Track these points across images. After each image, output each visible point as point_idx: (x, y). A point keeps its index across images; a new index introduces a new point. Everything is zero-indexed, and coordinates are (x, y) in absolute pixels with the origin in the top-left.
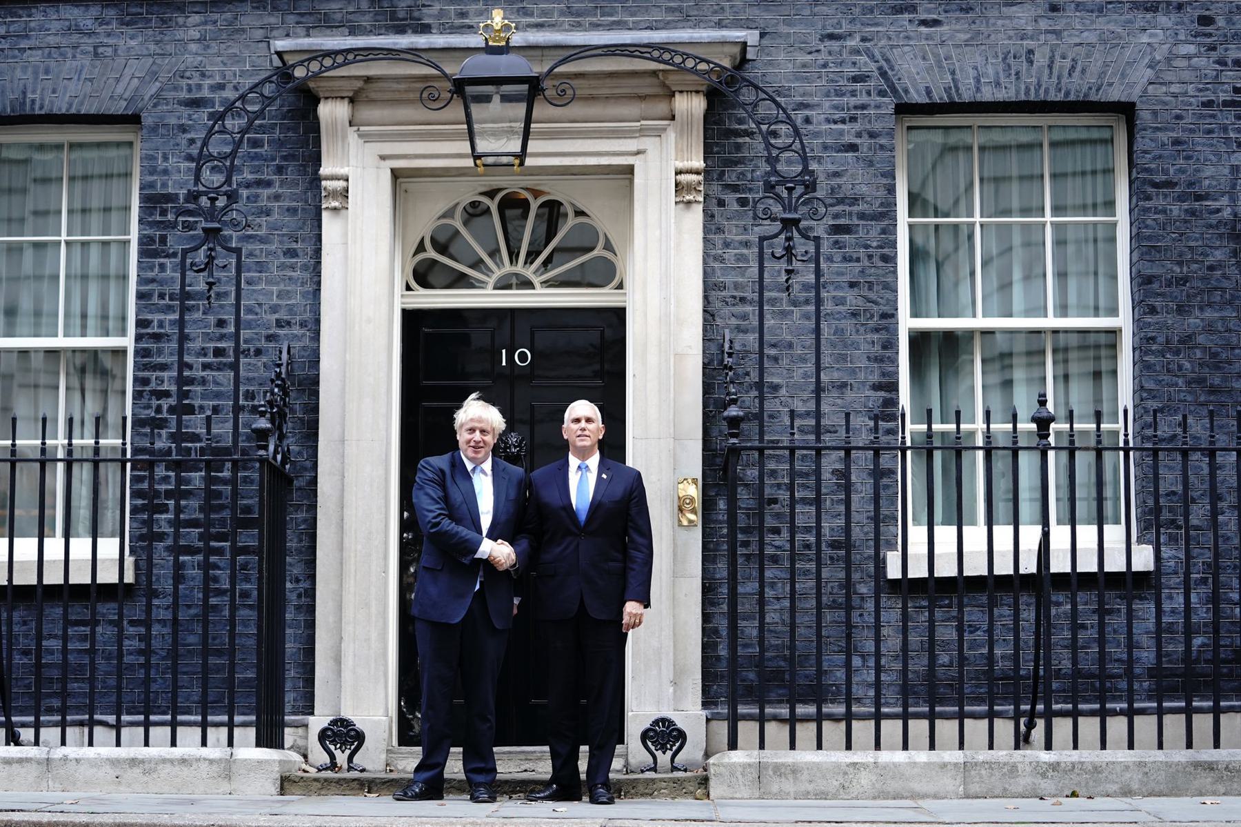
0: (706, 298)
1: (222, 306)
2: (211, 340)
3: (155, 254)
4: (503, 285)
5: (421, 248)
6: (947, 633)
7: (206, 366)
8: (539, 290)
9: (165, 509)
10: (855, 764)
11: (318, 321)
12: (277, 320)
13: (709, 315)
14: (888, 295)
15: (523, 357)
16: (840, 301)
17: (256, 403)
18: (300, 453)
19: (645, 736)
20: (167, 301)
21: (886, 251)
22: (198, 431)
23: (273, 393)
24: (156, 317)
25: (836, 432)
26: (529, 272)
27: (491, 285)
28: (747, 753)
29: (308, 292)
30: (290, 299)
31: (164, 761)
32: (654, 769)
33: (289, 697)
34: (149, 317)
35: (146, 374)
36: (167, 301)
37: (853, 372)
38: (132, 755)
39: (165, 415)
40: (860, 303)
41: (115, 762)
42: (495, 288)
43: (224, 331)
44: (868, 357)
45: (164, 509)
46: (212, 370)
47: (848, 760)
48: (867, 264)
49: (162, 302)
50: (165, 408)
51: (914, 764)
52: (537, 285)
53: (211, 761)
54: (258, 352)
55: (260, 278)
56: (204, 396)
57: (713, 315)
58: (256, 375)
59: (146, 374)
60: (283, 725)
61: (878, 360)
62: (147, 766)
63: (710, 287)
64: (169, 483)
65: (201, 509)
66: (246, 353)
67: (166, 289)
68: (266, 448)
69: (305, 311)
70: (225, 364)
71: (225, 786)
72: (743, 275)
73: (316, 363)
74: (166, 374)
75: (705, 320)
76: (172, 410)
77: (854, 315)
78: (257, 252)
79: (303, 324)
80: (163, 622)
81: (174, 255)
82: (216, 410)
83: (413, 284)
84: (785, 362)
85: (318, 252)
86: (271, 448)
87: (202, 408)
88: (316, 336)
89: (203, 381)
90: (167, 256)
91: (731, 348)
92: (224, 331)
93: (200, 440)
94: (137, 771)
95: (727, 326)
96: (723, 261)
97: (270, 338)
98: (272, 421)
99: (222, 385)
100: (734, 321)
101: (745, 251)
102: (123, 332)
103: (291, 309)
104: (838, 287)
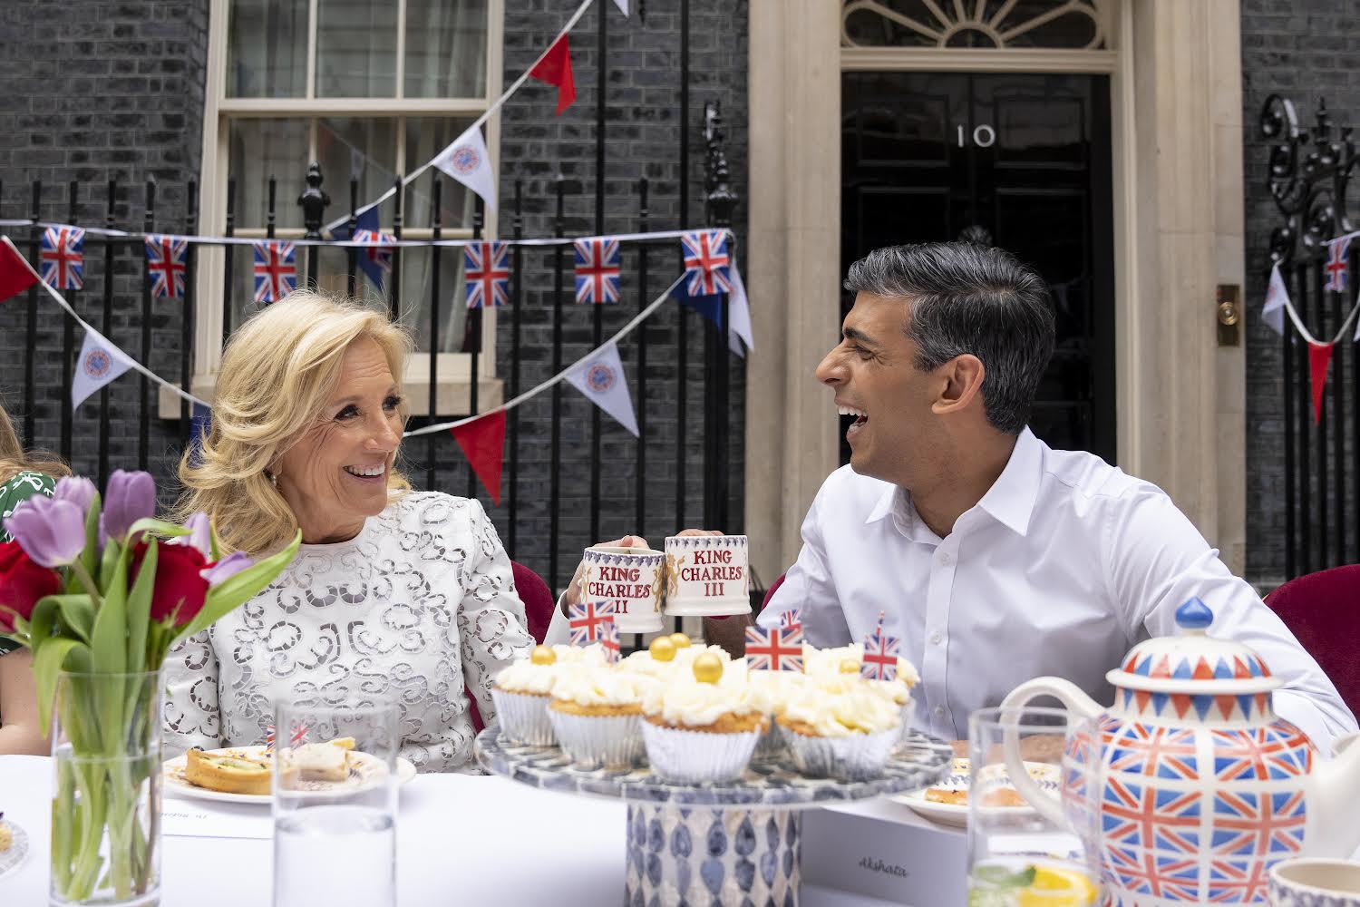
11: (744, 71)
17: (663, 180)
30: (706, 46)
34: (520, 67)
39: (542, 194)
45: (539, 317)
50: (543, 185)
55: (667, 19)
64: (547, 284)
66: (649, 115)
74: (544, 142)
79: (724, 79)
102: (483, 95)
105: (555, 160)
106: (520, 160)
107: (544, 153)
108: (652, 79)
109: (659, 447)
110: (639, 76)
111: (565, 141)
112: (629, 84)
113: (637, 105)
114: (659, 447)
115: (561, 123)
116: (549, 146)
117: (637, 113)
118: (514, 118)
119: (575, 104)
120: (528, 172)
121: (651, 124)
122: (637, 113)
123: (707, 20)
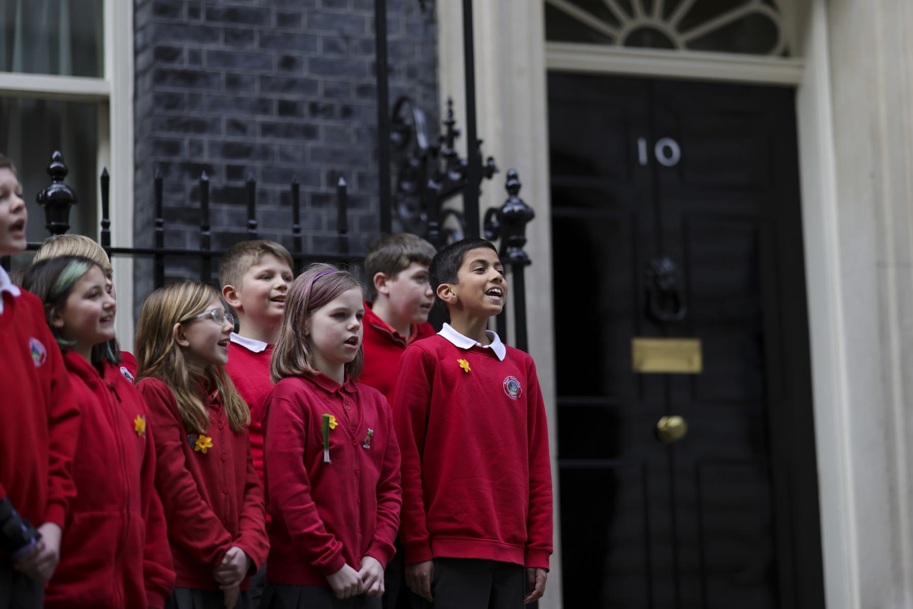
1: (289, 37)
2: (274, 88)
4: (636, 39)
7: (267, 129)
8: (683, 53)
20: (202, 20)
24: (187, 46)
26: (669, 28)
34: (175, 44)
35: (173, 135)
49: (195, 22)
54: (347, 112)
59: (173, 135)
66: (327, 111)
74: (205, 138)
79: (411, 73)
89: (265, 153)
105: (220, 162)
106: (177, 159)
108: (330, 68)
110: (315, 64)
111: (231, 139)
112: (303, 73)
113: (313, 98)
115: (225, 116)
116: (212, 145)
117: (315, 109)
118: (168, 107)
119: (242, 94)
121: (330, 123)
122: (315, 109)
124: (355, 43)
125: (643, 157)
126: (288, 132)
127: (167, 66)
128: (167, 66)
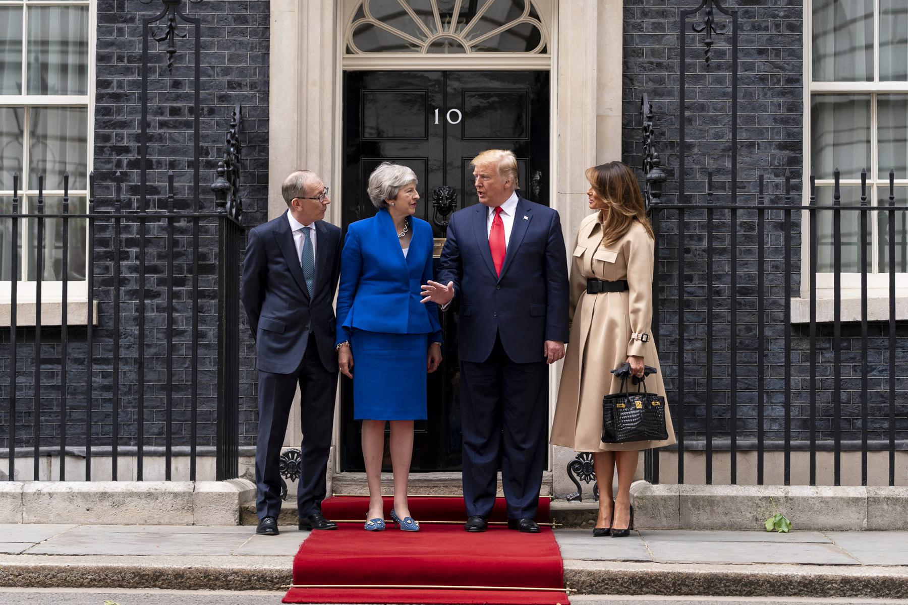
0: (625, 64)
2: (167, 100)
3: (113, 19)
4: (437, 46)
5: (360, 13)
6: (849, 374)
7: (162, 124)
9: (126, 256)
10: (767, 498)
11: (267, 83)
12: (229, 82)
13: (628, 80)
14: (794, 61)
15: (454, 116)
16: (750, 67)
17: (210, 158)
18: (250, 205)
19: (571, 467)
21: (792, 20)
22: (156, 184)
23: (229, 153)
24: (116, 78)
25: (744, 188)
26: (460, 37)
27: (424, 49)
28: (668, 486)
29: (257, 56)
30: (240, 62)
31: (131, 494)
32: (579, 498)
33: (242, 429)
34: (109, 78)
35: (107, 131)
36: (125, 63)
37: (760, 133)
38: (102, 490)
40: (767, 69)
41: (86, 496)
42: (428, 52)
43: (180, 91)
44: (775, 119)
46: (169, 127)
47: (760, 495)
48: (775, 32)
51: (822, 500)
52: (467, 48)
53: (176, 495)
54: (212, 112)
55: (212, 43)
56: (161, 153)
57: (631, 80)
58: (210, 132)
59: (107, 131)
60: (237, 454)
61: (784, 121)
62: (116, 498)
63: (628, 53)
64: (130, 233)
65: (160, 256)
67: (125, 52)
68: (223, 205)
69: (255, 74)
70: (180, 122)
71: (189, 518)
72: (659, 43)
73: (265, 121)
74: (125, 132)
75: (624, 84)
76: (133, 164)
77: (762, 79)
78: (210, 18)
79: (253, 86)
80: (126, 361)
81: (132, 20)
82: (172, 165)
83: (353, 47)
84: (697, 123)
85: (266, 18)
86: (228, 205)
87: (159, 163)
88: (265, 97)
89: (161, 138)
90: (125, 21)
91: (651, 112)
92: (180, 91)
93: (158, 193)
94: (107, 503)
95: (645, 90)
96: (641, 29)
97: (222, 98)
98: (229, 180)
99: (178, 142)
100: (651, 86)
101: (662, 20)
102: (82, 92)
103: (242, 72)
104: (747, 53)
105: (133, 145)
107: (125, 140)
109: (207, 346)
114: (207, 346)
116: (129, 135)
118: (104, 115)
120: (114, 153)
123: (241, 43)
124: (217, 70)
125: (437, 122)
126: (176, 125)
127: (103, 91)
128: (103, 91)
